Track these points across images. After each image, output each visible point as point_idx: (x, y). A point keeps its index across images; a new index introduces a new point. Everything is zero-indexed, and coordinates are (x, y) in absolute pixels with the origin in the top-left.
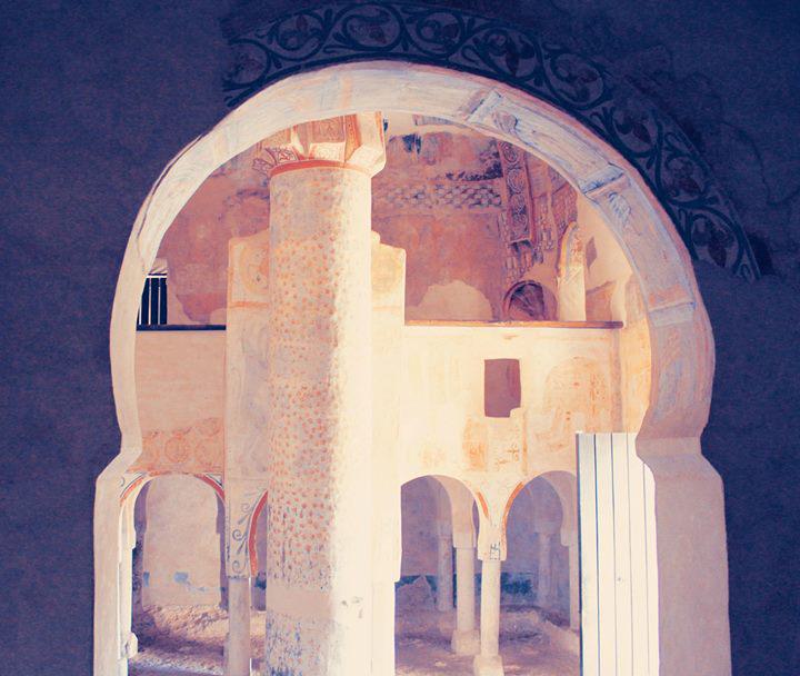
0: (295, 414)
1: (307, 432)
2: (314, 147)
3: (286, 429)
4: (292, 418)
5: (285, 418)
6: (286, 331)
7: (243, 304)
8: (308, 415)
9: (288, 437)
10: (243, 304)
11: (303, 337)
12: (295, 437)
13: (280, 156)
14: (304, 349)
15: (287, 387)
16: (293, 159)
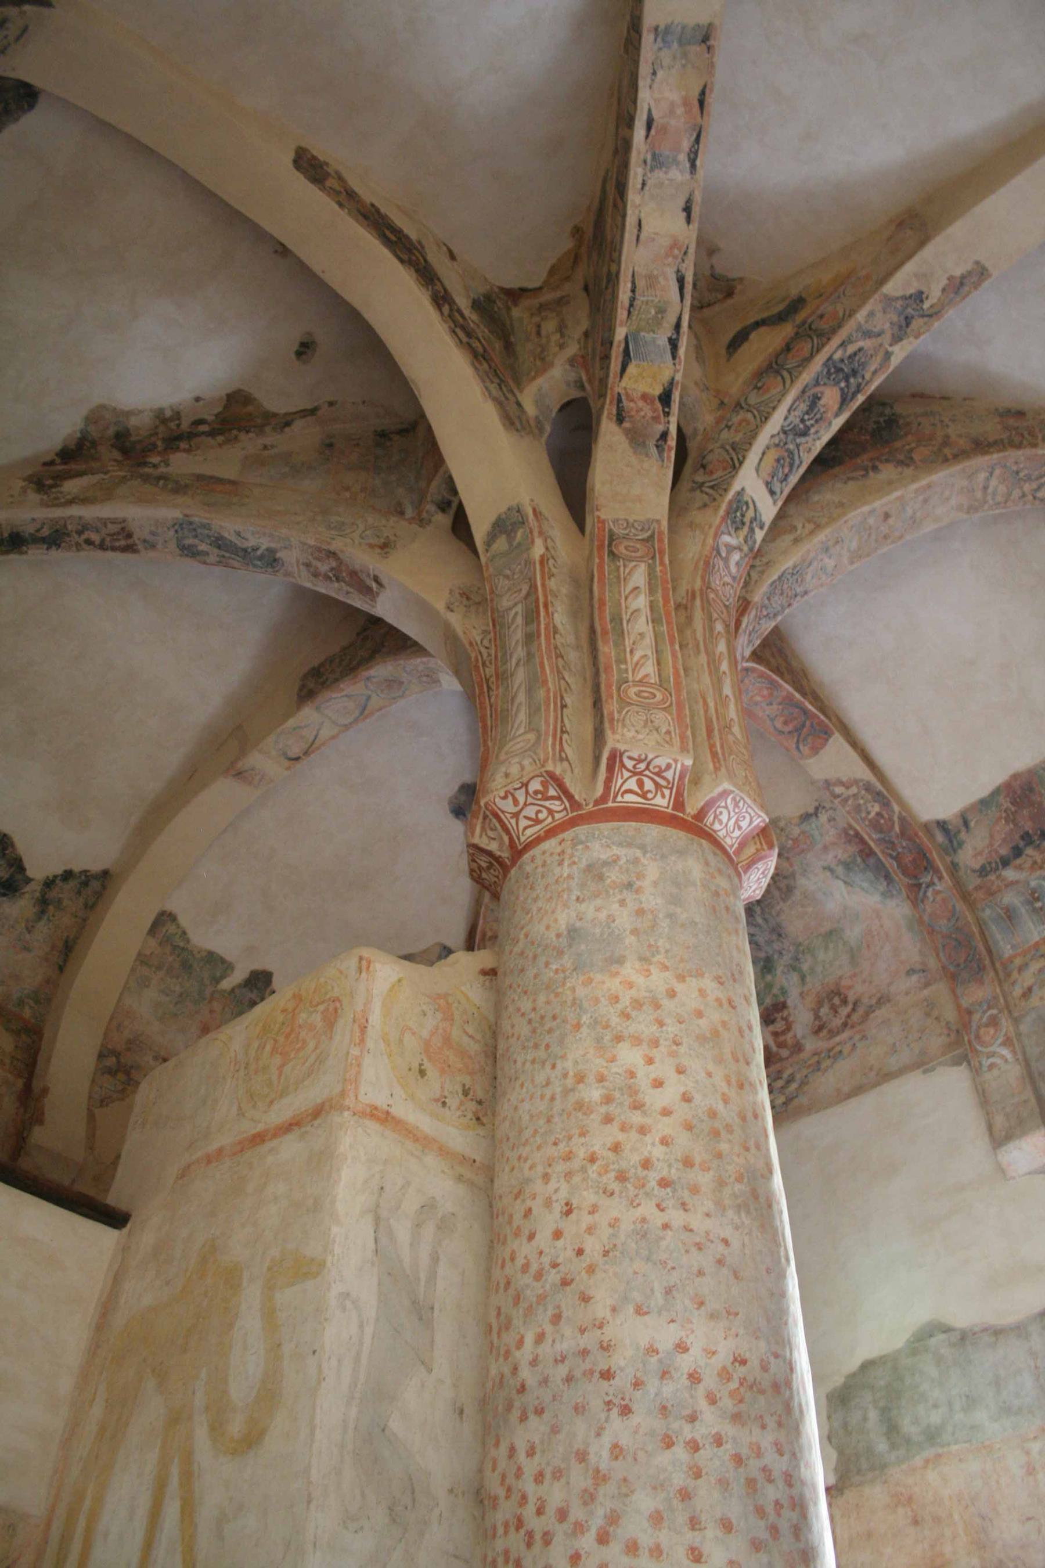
0: (718, 1441)
1: (760, 1512)
2: (725, 794)
3: (685, 1495)
4: (707, 1452)
5: (680, 1452)
6: (664, 1183)
7: (384, 1118)
8: (758, 1452)
9: (694, 1523)
10: (384, 1118)
11: (719, 1204)
12: (727, 1526)
13: (632, 784)
14: (726, 1242)
15: (682, 1347)
16: (662, 802)
